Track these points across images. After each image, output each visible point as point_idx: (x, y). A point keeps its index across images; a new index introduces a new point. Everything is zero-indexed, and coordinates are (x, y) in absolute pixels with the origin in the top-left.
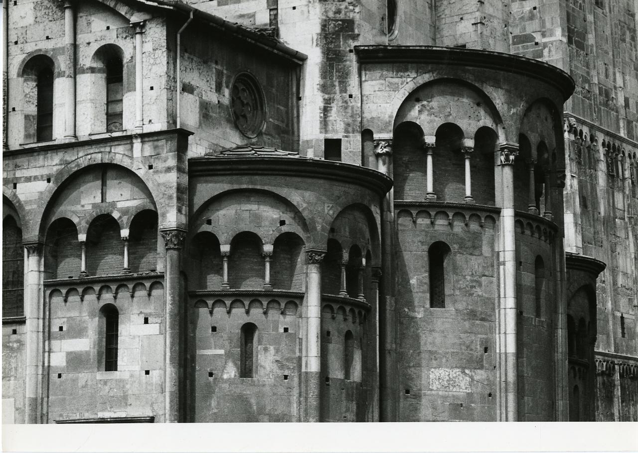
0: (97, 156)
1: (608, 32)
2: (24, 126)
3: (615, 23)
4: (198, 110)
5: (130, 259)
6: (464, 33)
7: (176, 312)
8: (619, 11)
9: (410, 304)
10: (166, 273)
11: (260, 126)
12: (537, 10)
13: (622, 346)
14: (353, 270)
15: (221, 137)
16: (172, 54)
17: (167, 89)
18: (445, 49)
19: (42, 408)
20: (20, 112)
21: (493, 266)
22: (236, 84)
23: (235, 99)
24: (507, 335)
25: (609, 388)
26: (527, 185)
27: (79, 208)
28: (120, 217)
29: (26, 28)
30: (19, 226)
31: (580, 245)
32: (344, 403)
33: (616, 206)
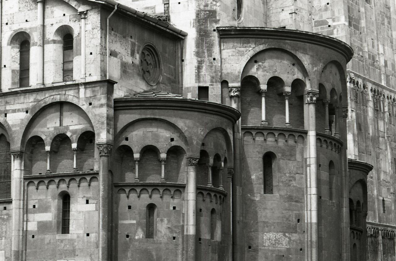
0: (57, 97)
1: (374, 19)
2: (11, 77)
3: (378, 13)
4: (120, 68)
5: (78, 162)
6: (285, 19)
7: (106, 196)
8: (380, 5)
9: (252, 192)
10: (100, 172)
11: (158, 78)
12: (330, 5)
13: (383, 218)
14: (216, 170)
15: (134, 85)
16: (104, 32)
17: (101, 54)
18: (273, 29)
19: (22, 257)
20: (8, 68)
21: (302, 167)
22: (144, 51)
23: (143, 60)
24: (312, 212)
25: (375, 245)
26: (324, 116)
27: (45, 129)
28: (71, 136)
29: (13, 15)
30: (8, 141)
31: (357, 154)
32: (211, 254)
33: (379, 129)
